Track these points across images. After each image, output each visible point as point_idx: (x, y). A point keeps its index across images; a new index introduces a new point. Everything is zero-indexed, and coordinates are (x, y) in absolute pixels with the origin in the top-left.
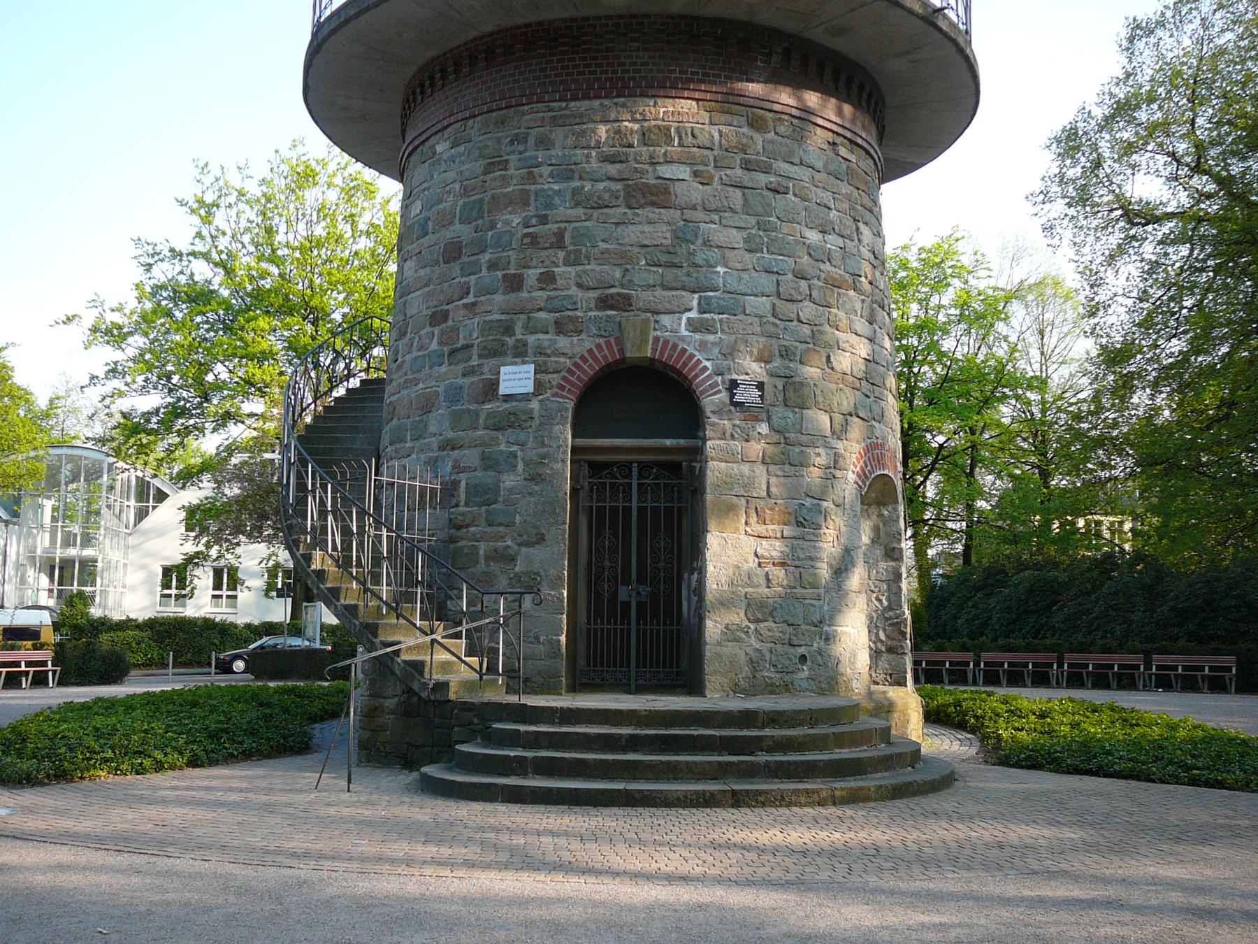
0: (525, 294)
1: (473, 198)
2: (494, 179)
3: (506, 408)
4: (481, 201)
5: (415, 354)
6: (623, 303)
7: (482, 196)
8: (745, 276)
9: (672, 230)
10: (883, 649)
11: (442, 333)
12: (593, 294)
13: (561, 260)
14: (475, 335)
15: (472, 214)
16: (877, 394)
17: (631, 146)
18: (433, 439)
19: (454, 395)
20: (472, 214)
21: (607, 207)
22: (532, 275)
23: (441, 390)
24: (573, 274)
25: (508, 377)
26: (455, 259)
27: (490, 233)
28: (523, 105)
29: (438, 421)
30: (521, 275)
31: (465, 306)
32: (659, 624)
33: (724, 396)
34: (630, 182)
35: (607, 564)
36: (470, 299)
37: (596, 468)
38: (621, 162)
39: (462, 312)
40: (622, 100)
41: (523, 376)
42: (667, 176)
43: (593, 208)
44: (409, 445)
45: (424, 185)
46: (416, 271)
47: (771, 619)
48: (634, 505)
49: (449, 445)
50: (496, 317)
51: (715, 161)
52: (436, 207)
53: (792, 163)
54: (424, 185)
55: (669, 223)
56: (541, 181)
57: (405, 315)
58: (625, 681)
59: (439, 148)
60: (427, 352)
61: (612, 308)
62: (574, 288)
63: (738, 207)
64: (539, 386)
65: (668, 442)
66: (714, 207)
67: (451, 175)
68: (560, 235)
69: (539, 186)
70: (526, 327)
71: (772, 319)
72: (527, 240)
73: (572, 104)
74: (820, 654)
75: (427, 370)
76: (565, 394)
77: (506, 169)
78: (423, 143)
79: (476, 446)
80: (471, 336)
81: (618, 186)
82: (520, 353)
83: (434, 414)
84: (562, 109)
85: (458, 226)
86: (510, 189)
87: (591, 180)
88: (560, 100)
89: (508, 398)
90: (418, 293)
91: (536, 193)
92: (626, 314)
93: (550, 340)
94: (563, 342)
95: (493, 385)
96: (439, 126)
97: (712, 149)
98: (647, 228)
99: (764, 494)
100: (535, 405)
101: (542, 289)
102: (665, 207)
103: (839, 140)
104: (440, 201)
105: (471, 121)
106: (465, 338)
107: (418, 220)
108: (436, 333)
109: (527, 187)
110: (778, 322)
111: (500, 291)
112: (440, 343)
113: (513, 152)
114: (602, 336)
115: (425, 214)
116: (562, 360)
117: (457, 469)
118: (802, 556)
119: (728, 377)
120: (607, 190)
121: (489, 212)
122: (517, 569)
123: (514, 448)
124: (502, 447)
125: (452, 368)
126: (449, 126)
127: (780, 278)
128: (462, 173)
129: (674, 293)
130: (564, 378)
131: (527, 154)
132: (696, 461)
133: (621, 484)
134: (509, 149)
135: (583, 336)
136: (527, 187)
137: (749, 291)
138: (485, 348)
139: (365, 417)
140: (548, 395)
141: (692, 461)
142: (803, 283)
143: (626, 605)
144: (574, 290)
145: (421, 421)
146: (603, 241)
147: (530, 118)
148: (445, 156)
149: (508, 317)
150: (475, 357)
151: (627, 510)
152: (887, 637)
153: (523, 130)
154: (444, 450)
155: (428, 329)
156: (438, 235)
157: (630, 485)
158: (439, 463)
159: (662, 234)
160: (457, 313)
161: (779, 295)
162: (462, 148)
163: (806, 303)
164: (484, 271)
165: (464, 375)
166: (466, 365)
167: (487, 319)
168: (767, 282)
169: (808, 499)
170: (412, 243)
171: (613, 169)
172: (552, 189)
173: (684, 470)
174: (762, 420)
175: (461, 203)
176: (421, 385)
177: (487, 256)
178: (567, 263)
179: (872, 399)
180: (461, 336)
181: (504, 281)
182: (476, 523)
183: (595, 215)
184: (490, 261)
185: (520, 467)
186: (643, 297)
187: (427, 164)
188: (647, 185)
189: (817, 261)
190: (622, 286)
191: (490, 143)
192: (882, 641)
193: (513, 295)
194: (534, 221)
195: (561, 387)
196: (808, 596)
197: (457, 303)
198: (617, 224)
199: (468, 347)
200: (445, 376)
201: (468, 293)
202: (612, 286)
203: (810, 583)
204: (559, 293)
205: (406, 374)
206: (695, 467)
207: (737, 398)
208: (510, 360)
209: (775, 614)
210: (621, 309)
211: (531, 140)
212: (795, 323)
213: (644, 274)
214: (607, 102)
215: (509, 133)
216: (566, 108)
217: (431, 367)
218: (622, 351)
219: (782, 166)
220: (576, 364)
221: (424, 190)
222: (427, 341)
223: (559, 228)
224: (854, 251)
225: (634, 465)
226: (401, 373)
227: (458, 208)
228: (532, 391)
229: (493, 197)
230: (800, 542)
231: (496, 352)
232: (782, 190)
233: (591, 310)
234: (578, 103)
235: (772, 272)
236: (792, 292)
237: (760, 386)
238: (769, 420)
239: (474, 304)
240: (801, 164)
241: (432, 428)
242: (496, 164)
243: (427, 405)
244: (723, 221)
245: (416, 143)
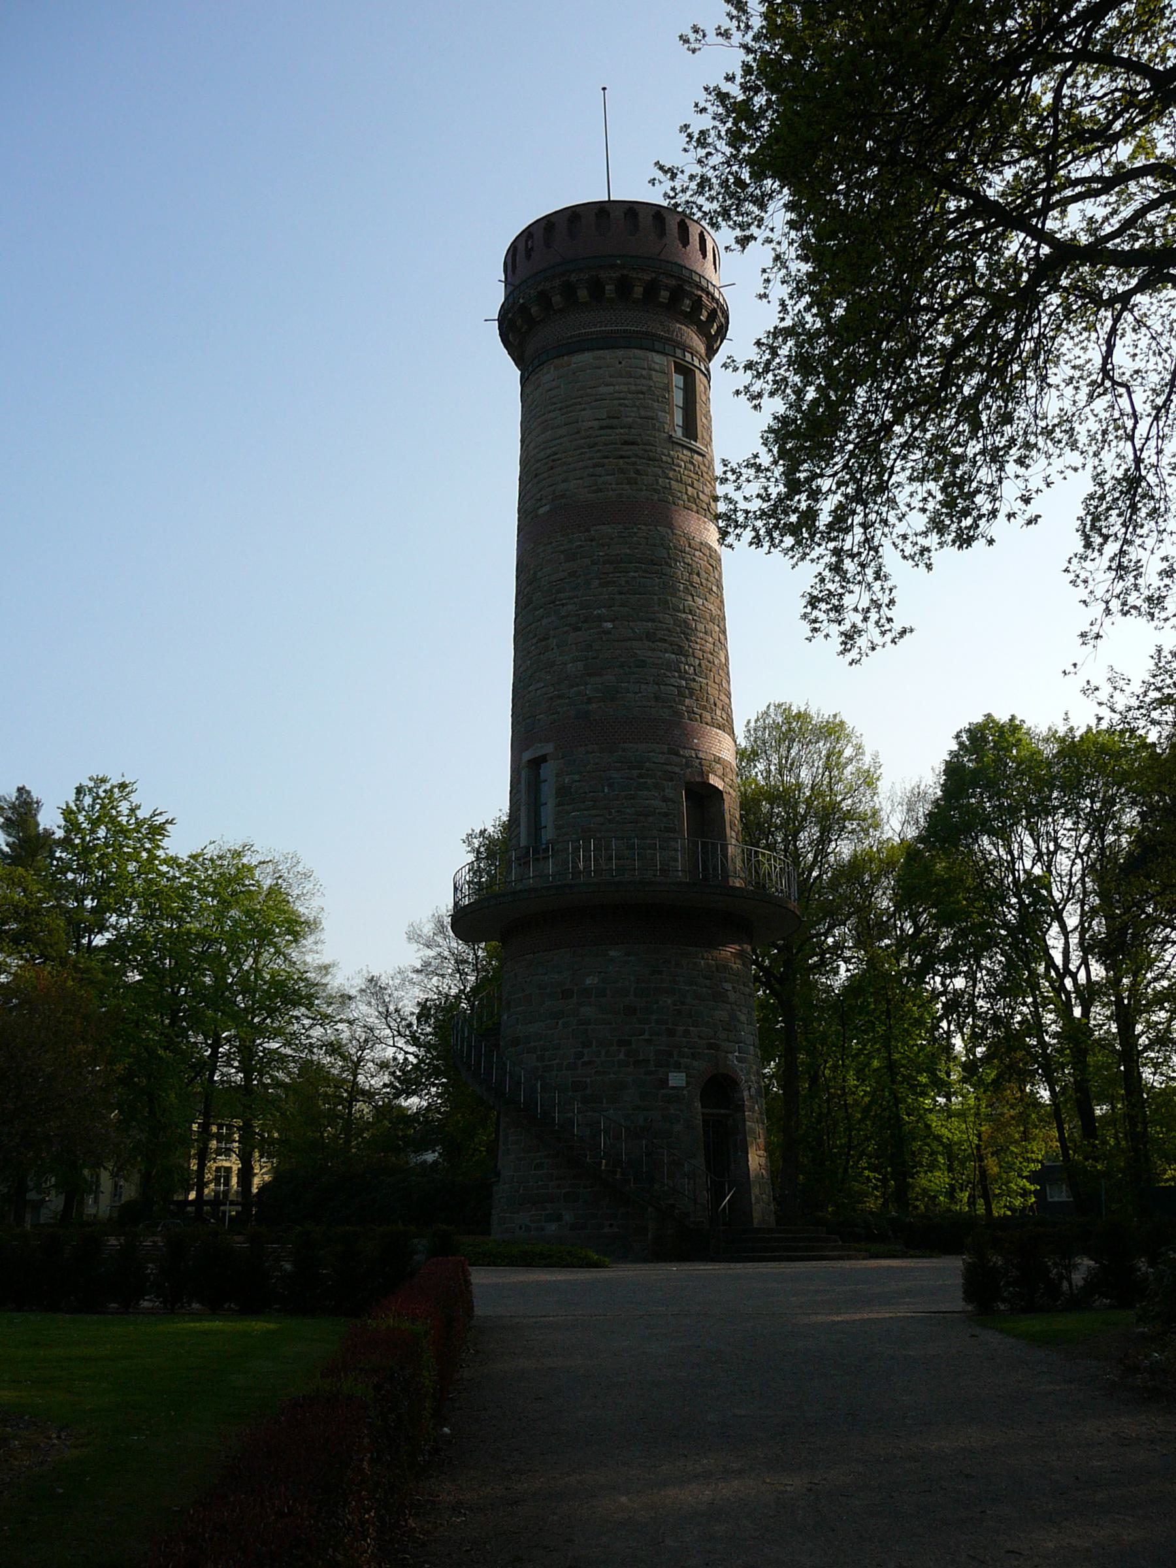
12: (704, 1042)
31: (645, 1040)
64: (688, 1083)
82: (678, 1067)
89: (673, 1088)
94: (695, 1063)
124: (672, 1111)
144: (697, 1040)
177: (654, 1017)
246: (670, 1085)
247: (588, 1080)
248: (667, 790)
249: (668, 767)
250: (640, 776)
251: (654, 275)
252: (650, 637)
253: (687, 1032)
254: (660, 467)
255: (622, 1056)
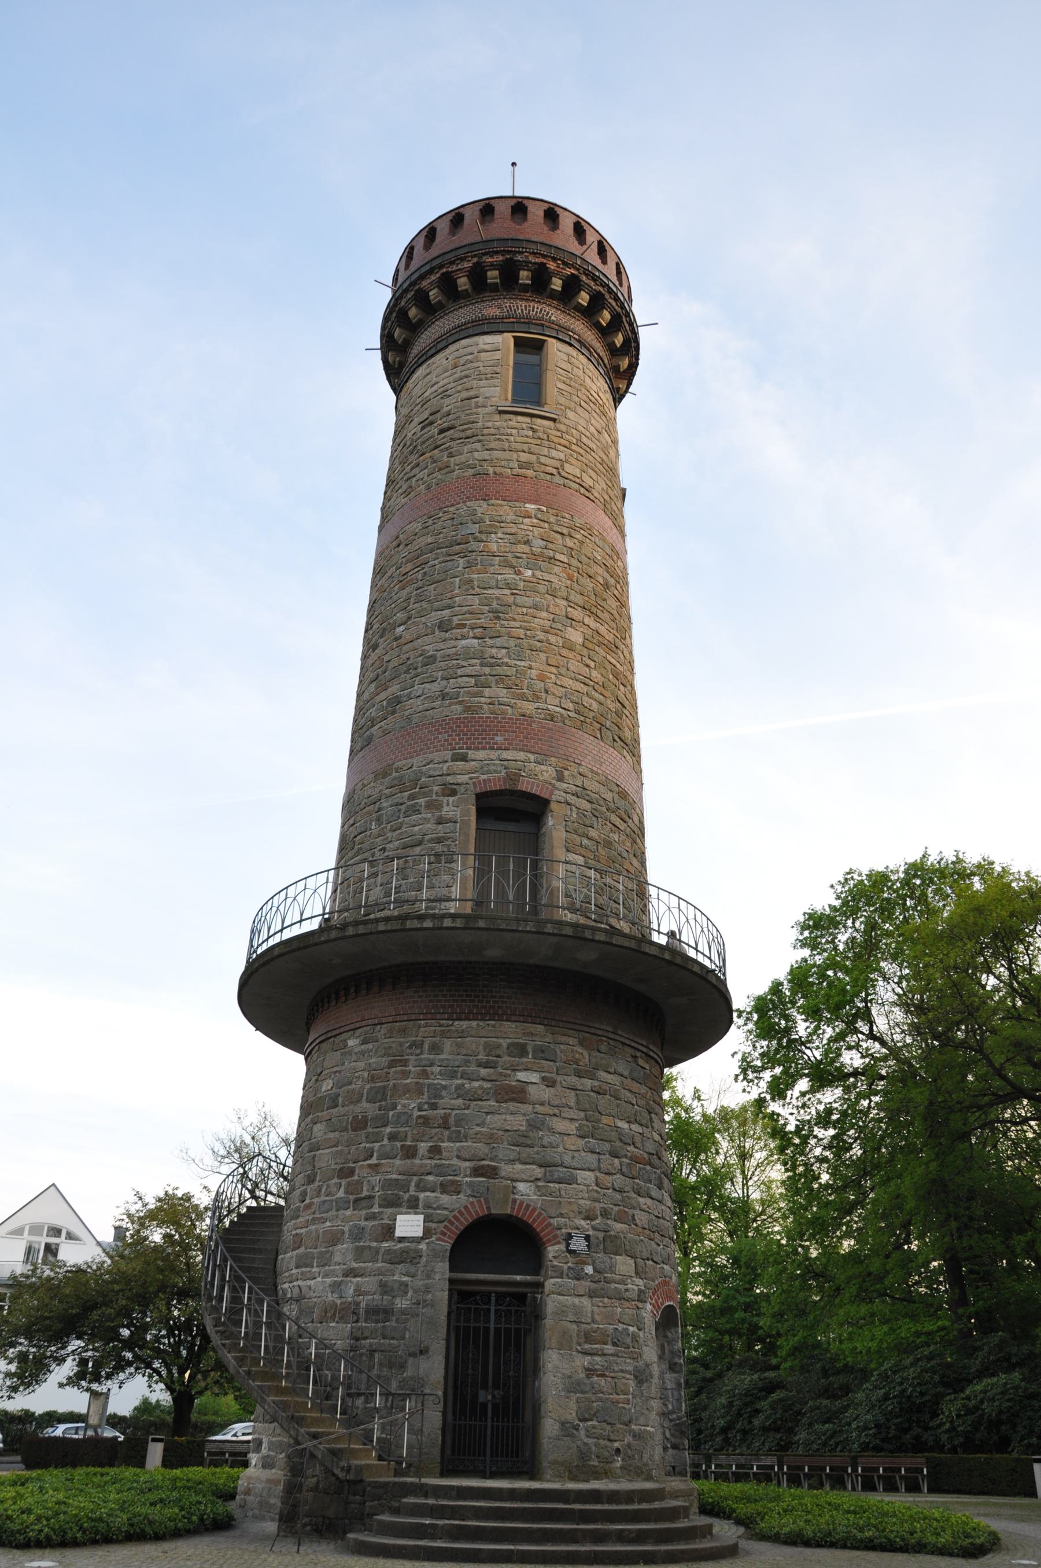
0: (417, 1161)
1: (377, 1085)
2: (396, 1072)
3: (401, 1248)
4: (384, 1087)
5: (323, 1198)
6: (490, 1173)
7: (386, 1083)
8: (576, 1154)
9: (527, 1120)
10: (669, 1446)
11: (349, 1184)
12: (467, 1164)
13: (446, 1137)
14: (377, 1189)
15: (379, 1095)
16: (664, 1243)
17: (499, 1056)
18: (338, 1267)
19: (358, 1234)
20: (379, 1095)
21: (481, 1100)
22: (423, 1147)
23: (346, 1229)
24: (455, 1149)
25: (404, 1223)
26: (361, 1129)
27: (391, 1113)
28: (420, 1020)
29: (343, 1252)
30: (415, 1146)
31: (370, 1166)
32: (508, 1421)
33: (562, 1247)
34: (498, 1083)
35: (470, 1371)
36: (374, 1161)
37: (461, 1293)
38: (491, 1067)
39: (367, 1170)
40: (493, 1022)
41: (414, 1223)
42: (525, 1080)
43: (470, 1100)
44: (314, 1270)
45: (335, 1069)
46: (325, 1133)
47: (595, 1418)
48: (492, 1326)
49: (351, 1273)
50: (394, 1176)
51: (557, 1070)
52: (346, 1087)
53: (609, 1073)
54: (335, 1069)
55: (524, 1115)
56: (433, 1077)
57: (314, 1166)
58: (481, 1468)
59: (351, 1043)
60: (334, 1198)
61: (482, 1175)
62: (455, 1159)
63: (572, 1104)
64: (427, 1232)
65: (518, 1278)
66: (556, 1103)
67: (361, 1065)
68: (445, 1118)
69: (430, 1081)
70: (417, 1185)
71: (596, 1188)
72: (422, 1121)
73: (456, 1023)
74: (630, 1448)
75: (333, 1213)
76: (446, 1239)
77: (405, 1066)
78: (335, 1036)
79: (375, 1275)
80: (373, 1189)
81: (486, 1085)
82: (413, 1206)
83: (339, 1247)
84: (448, 1026)
85: (364, 1104)
86: (408, 1081)
87: (469, 1079)
88: (448, 1019)
89: (402, 1239)
90: (326, 1151)
91: (429, 1085)
92: (493, 1181)
93: (436, 1197)
94: (445, 1199)
95: (390, 1229)
96: (352, 1026)
97: (555, 1062)
98: (509, 1117)
99: (589, 1320)
100: (423, 1246)
101: (430, 1158)
102: (522, 1103)
103: (639, 1054)
104: (351, 1084)
105: (379, 1027)
106: (368, 1190)
107: (329, 1094)
108: (343, 1184)
109: (421, 1081)
110: (600, 1190)
111: (398, 1157)
112: (346, 1192)
113: (412, 1054)
114: (474, 1196)
115: (334, 1090)
116: (445, 1212)
117: (358, 1292)
118: (616, 1369)
119: (564, 1231)
120: (481, 1087)
121: (391, 1097)
122: (405, 1375)
123: (405, 1279)
124: (396, 1278)
125: (356, 1212)
126: (360, 1028)
127: (602, 1157)
128: (370, 1064)
129: (528, 1166)
130: (446, 1227)
131: (423, 1056)
132: (538, 1293)
133: (482, 1309)
134: (408, 1051)
135: (461, 1196)
136: (421, 1081)
137: (579, 1166)
138: (384, 1199)
139: (259, 1240)
140: (433, 1239)
141: (535, 1293)
142: (616, 1161)
143: (484, 1406)
145: (327, 1252)
146: (478, 1125)
147: (426, 1031)
148: (356, 1050)
149: (404, 1177)
150: (377, 1206)
151: (487, 1330)
152: (672, 1435)
153: (419, 1038)
154: (347, 1276)
155: (336, 1180)
156: (347, 1108)
157: (489, 1310)
158: (343, 1287)
159: (518, 1122)
160: (361, 1170)
161: (599, 1169)
162: (370, 1046)
163: (618, 1176)
164: (386, 1142)
165: (366, 1219)
166: (368, 1211)
167: (387, 1177)
168: (592, 1159)
169: (621, 1325)
170: (323, 1111)
171: (483, 1072)
172: (441, 1085)
173: (529, 1301)
174: (589, 1264)
175: (368, 1086)
176: (328, 1224)
177: (388, 1130)
178: (450, 1140)
179: (661, 1247)
180: (365, 1189)
181: (402, 1150)
182: (373, 1336)
183: (472, 1105)
184: (390, 1133)
185: (410, 1294)
186: (506, 1170)
187: (338, 1053)
188: (510, 1086)
189: (625, 1144)
190: (491, 1160)
191: (394, 1045)
192: (668, 1439)
193: (408, 1161)
194: (426, 1107)
195: (444, 1234)
196: (621, 1401)
197: (362, 1163)
198: (487, 1113)
199: (370, 1197)
200: (350, 1218)
201: (372, 1156)
202: (483, 1159)
203: (622, 1391)
204: (444, 1162)
205: (314, 1213)
206: (537, 1298)
207: (572, 1247)
208: (404, 1210)
209: (598, 1415)
210: (489, 1177)
211: (426, 1046)
212: (610, 1191)
213: (504, 1150)
214: (481, 1023)
215: (409, 1039)
216: (452, 1025)
217: (337, 1210)
218: (489, 1208)
219: (602, 1075)
220: (455, 1217)
221: (336, 1072)
222: (335, 1189)
223: (445, 1113)
224: (649, 1136)
225: (493, 1295)
226: (308, 1212)
227: (365, 1090)
228: (421, 1235)
229: (394, 1086)
230: (615, 1358)
231: (394, 1203)
232: (602, 1091)
233: (467, 1176)
234: (462, 1023)
235: (596, 1153)
236: (609, 1167)
237: (587, 1238)
238: (593, 1264)
239: (377, 1165)
240: (615, 1073)
241: (338, 1258)
242: (398, 1061)
243: (334, 1239)
244: (562, 1114)
245: (329, 1035)
246: (398, 1233)
247: (303, 1230)
248: (446, 809)
249: (449, 778)
250: (412, 797)
251: (475, 260)
252: (444, 626)
253: (435, 1151)
254: (479, 441)
255: (341, 1194)
